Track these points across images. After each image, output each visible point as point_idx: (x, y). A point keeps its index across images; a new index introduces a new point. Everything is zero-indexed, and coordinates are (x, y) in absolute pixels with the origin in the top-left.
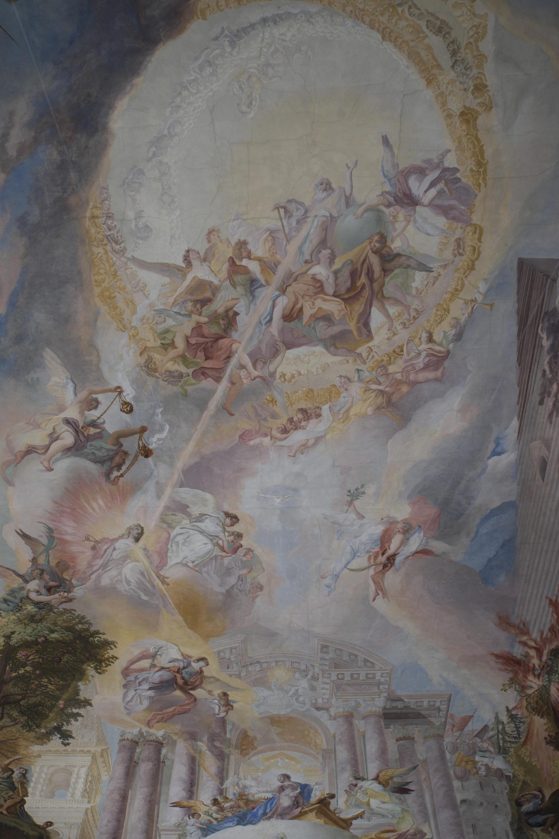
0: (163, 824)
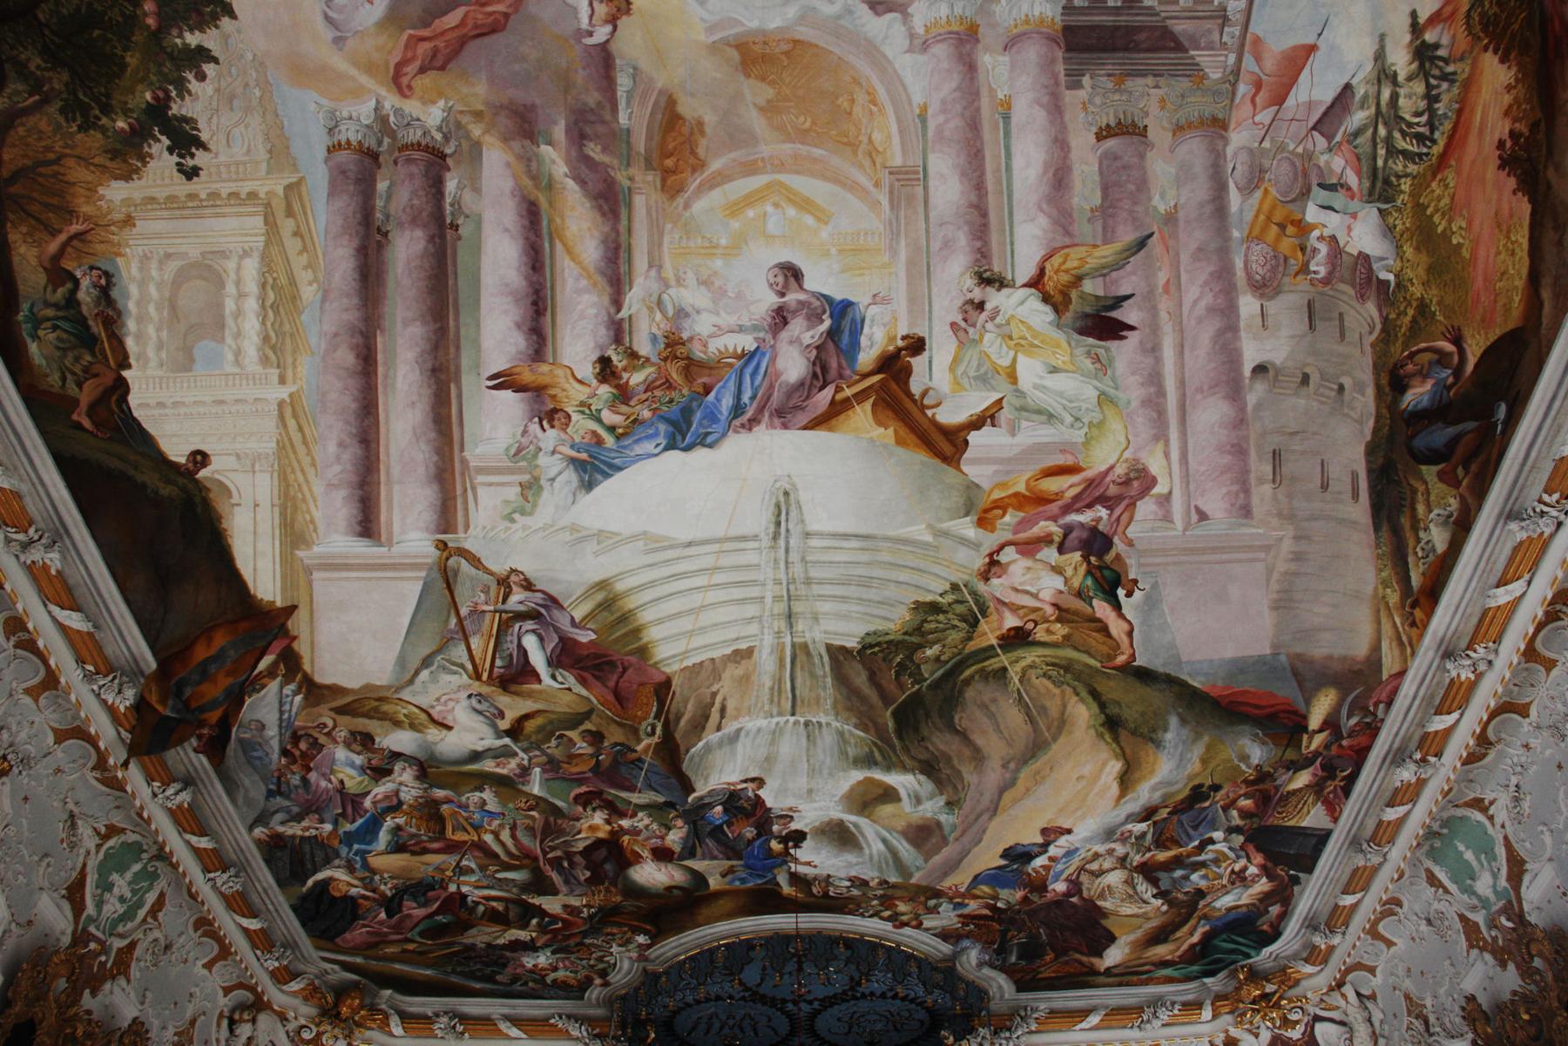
0: (478, 451)
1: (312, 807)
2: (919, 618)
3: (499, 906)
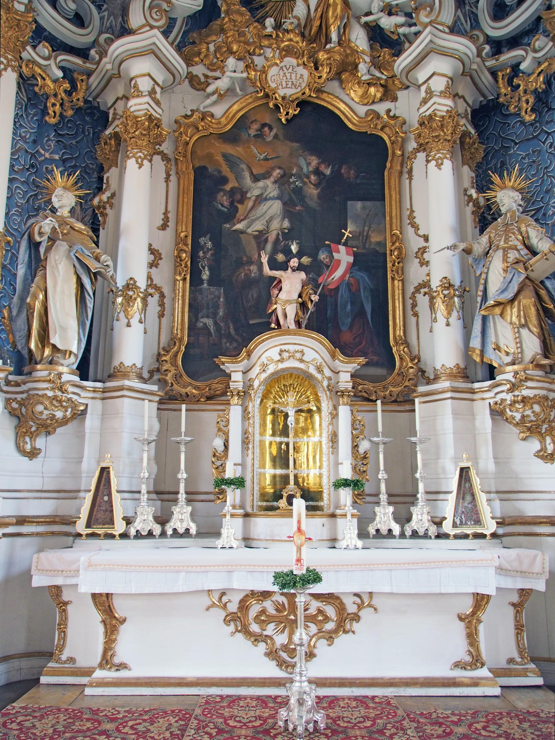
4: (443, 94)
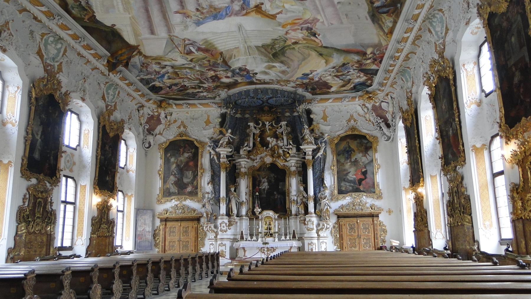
1: (149, 73)
2: (273, 41)
3: (194, 86)
4: (294, 166)
